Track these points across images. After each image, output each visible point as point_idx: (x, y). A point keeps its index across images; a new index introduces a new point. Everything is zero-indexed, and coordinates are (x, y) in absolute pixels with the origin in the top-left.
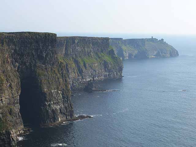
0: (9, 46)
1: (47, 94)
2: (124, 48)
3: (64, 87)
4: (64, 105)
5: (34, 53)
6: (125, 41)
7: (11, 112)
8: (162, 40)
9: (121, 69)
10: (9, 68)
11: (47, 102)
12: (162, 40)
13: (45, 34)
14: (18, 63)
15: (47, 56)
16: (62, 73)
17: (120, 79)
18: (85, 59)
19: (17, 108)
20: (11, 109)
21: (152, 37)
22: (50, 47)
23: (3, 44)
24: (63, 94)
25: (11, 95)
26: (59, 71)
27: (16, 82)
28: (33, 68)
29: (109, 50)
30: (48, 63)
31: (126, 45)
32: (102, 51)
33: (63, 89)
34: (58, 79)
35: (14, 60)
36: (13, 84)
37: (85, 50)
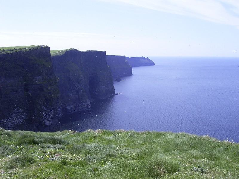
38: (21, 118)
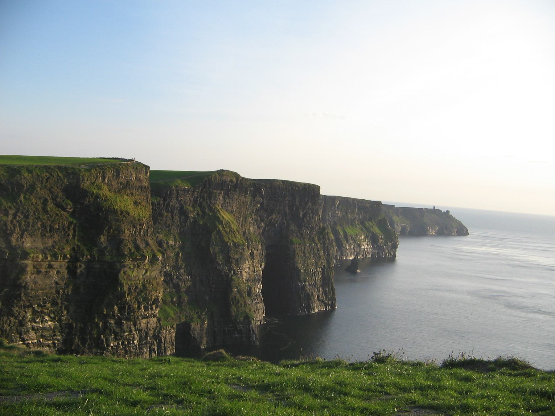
0: (254, 198)
1: (302, 271)
2: (395, 218)
3: (325, 264)
4: (323, 288)
5: (287, 211)
6: (398, 209)
7: (249, 293)
8: (448, 212)
9: (395, 247)
10: (252, 229)
11: (301, 283)
12: (448, 212)
13: (305, 184)
14: (264, 223)
15: (305, 215)
16: (324, 243)
17: (392, 259)
18: (348, 230)
19: (258, 288)
20: (250, 288)
22: (310, 204)
23: (246, 194)
24: (323, 273)
25: (251, 268)
26: (319, 240)
27: (259, 249)
29: (380, 218)
30: (305, 227)
31: (398, 216)
32: (370, 220)
33: (324, 266)
34: (318, 250)
35: (259, 219)
36: (255, 252)
37: (348, 216)
38: (49, 346)
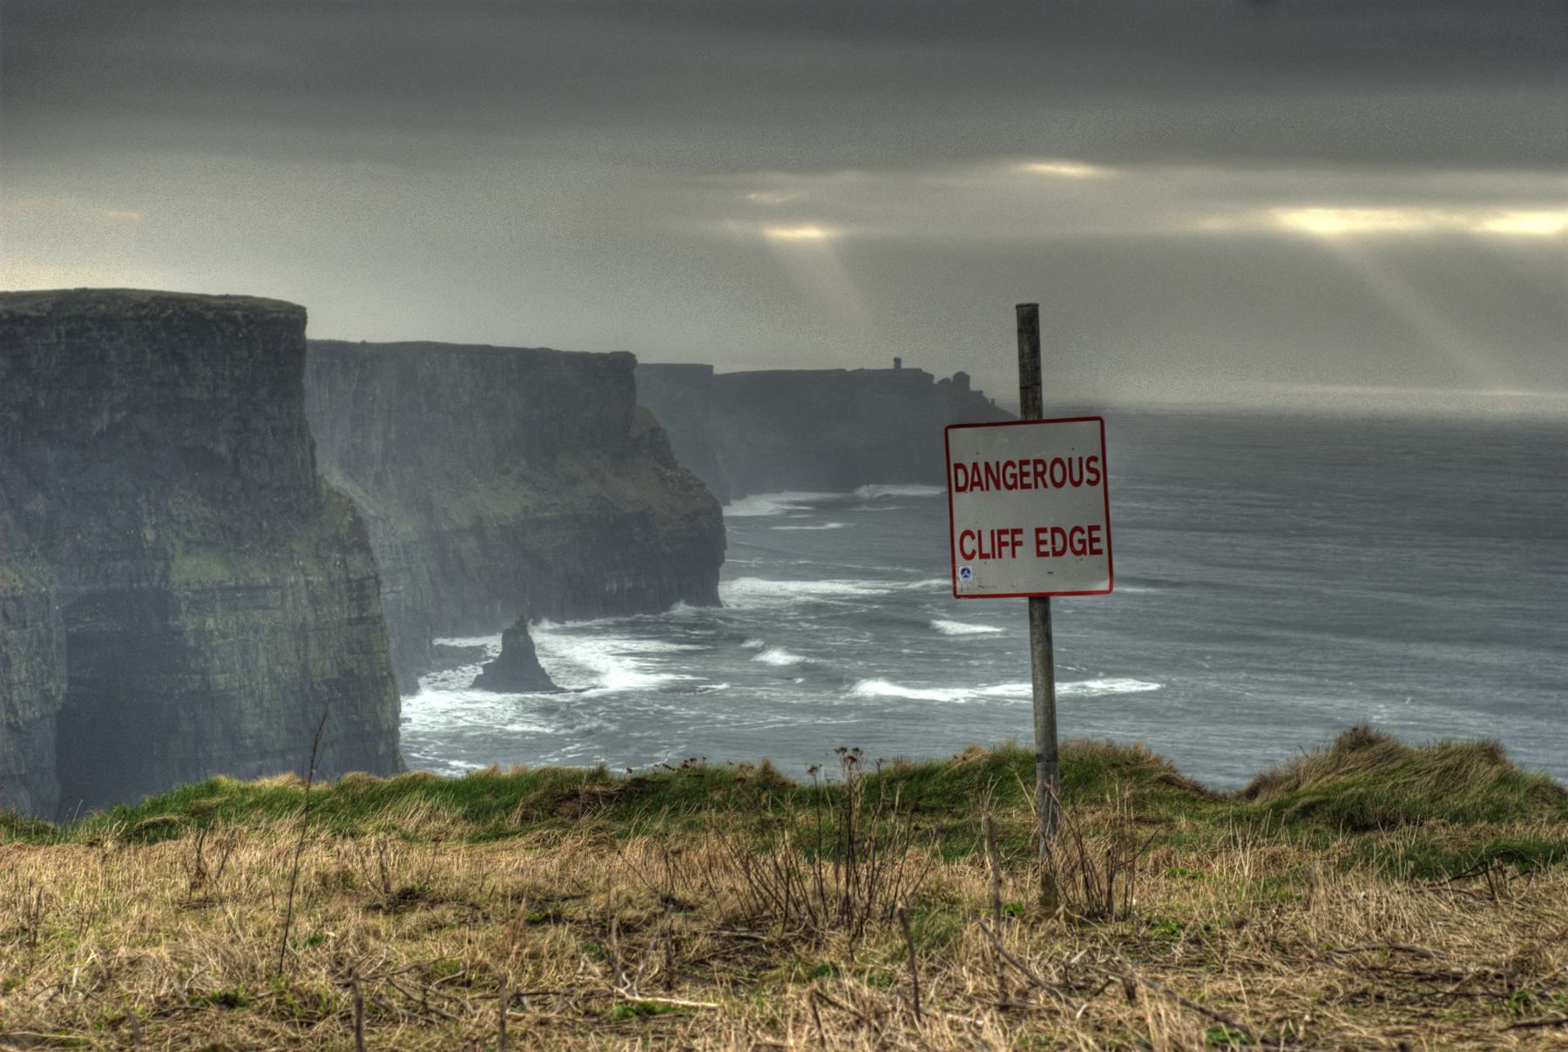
8: (962, 378)
12: (962, 378)
21: (898, 361)
28: (150, 535)
